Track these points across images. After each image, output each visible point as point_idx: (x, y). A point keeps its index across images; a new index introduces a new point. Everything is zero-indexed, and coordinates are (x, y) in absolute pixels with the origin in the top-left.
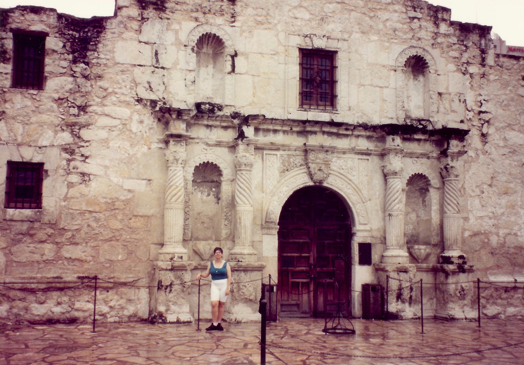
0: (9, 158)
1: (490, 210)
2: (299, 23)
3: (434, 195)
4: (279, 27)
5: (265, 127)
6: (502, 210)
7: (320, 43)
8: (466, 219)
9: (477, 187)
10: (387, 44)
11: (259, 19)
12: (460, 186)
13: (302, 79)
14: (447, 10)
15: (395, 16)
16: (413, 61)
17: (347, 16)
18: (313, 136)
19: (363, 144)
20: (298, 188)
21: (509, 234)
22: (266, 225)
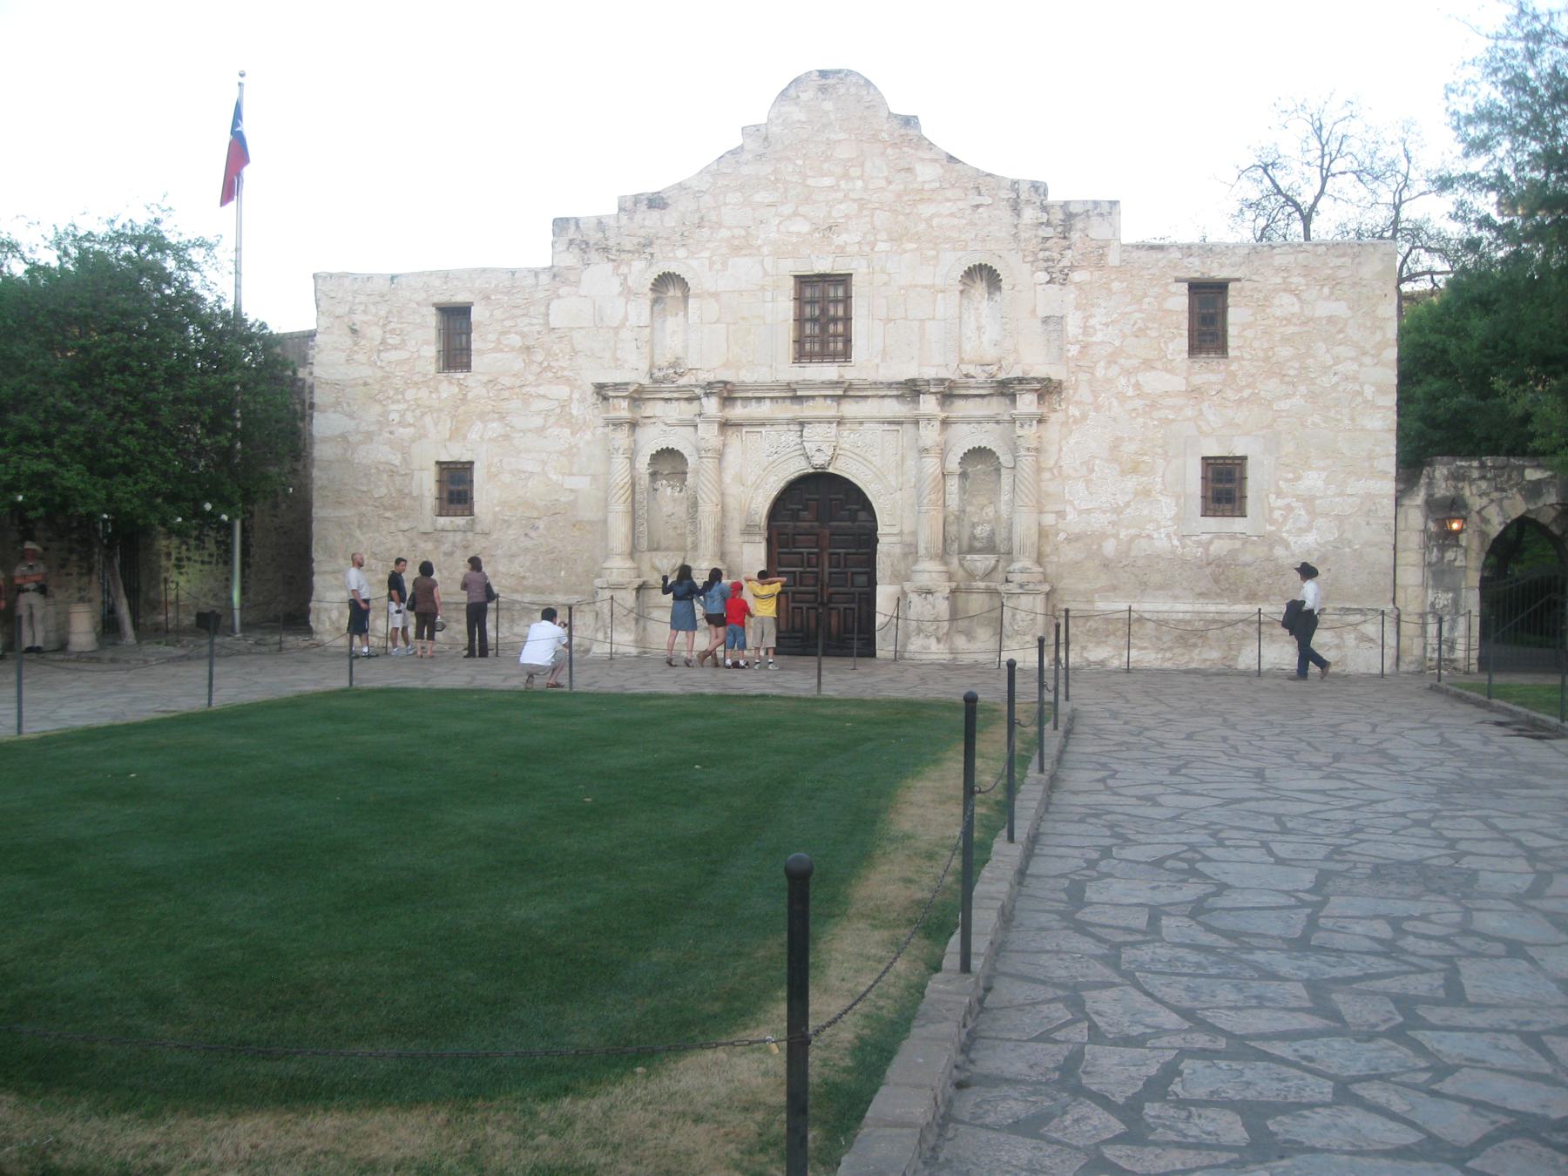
0: (437, 459)
1: (1104, 499)
2: (794, 240)
3: (1006, 478)
4: (765, 250)
5: (742, 395)
6: (1127, 499)
7: (823, 266)
8: (1061, 514)
9: (1082, 463)
10: (933, 253)
11: (736, 242)
12: (1051, 463)
13: (800, 320)
14: (1038, 188)
15: (948, 207)
16: (985, 273)
17: (868, 219)
18: (811, 403)
19: (893, 408)
20: (792, 477)
21: (1139, 536)
22: (748, 530)
